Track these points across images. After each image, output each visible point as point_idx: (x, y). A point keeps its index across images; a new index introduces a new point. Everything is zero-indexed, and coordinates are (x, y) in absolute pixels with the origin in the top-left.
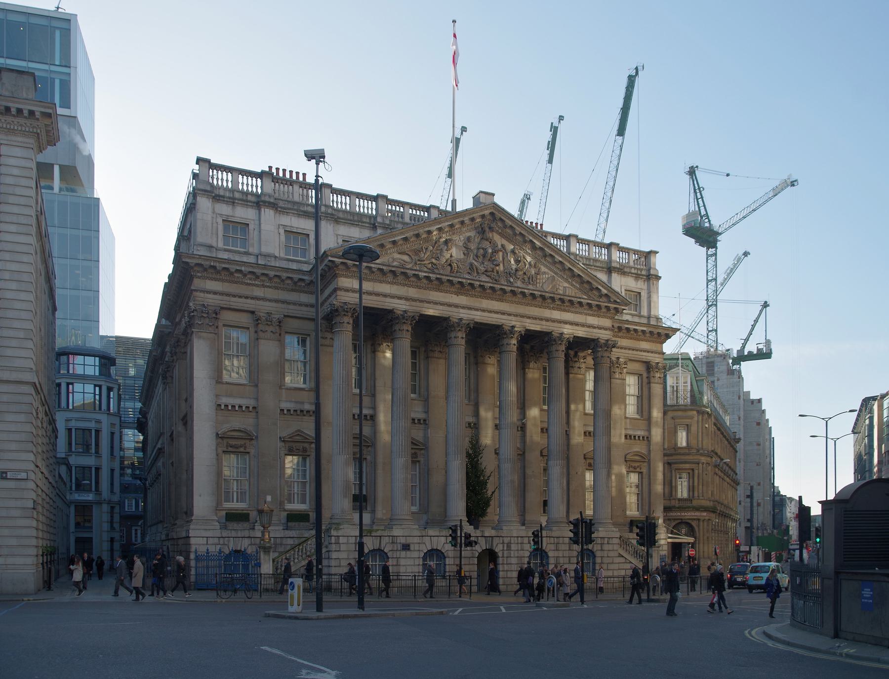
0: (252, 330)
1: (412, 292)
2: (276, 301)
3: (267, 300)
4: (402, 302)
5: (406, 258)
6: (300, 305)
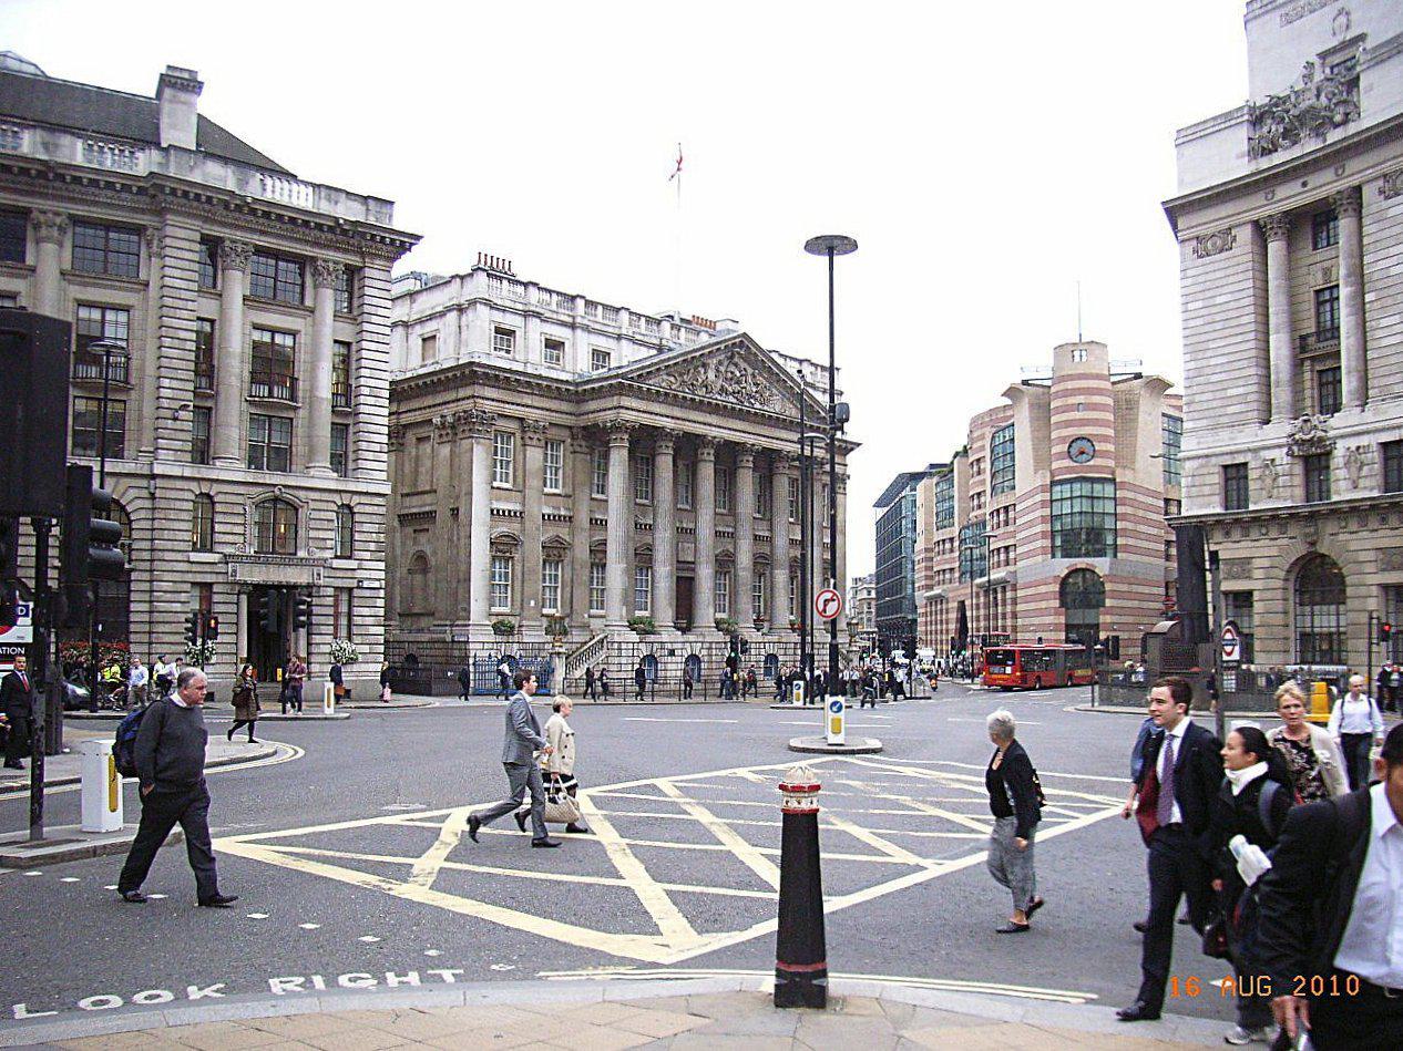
0: (518, 435)
1: (677, 412)
2: (542, 409)
3: (535, 410)
4: (669, 420)
5: (672, 379)
6: (561, 413)
